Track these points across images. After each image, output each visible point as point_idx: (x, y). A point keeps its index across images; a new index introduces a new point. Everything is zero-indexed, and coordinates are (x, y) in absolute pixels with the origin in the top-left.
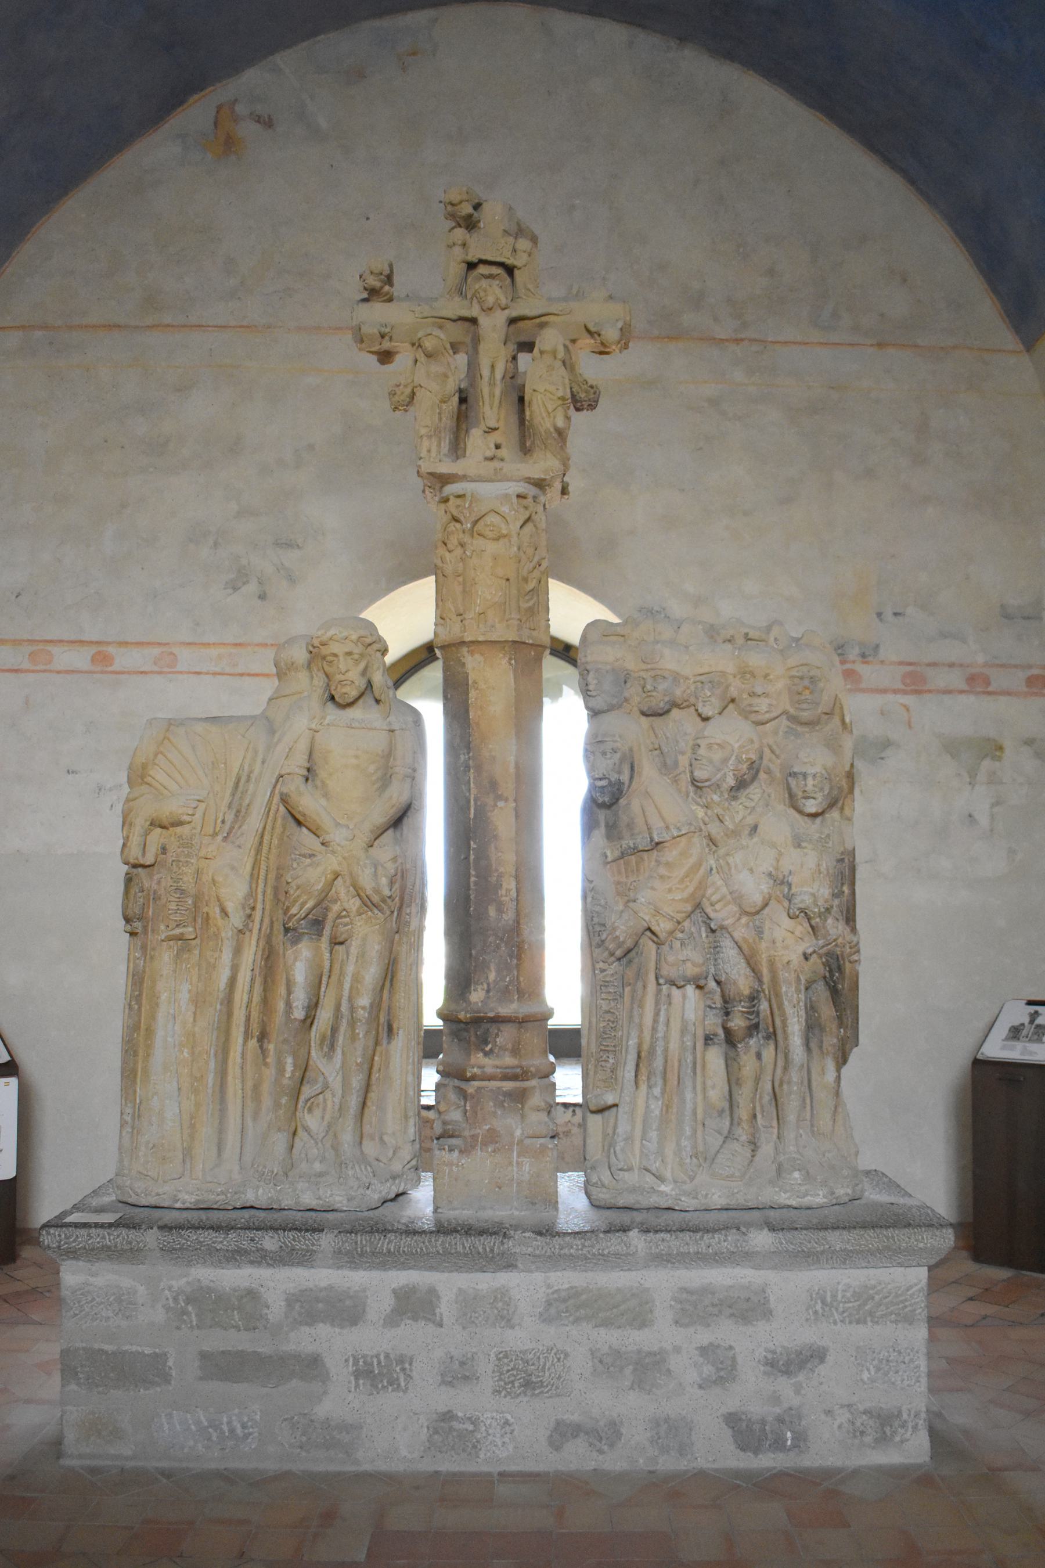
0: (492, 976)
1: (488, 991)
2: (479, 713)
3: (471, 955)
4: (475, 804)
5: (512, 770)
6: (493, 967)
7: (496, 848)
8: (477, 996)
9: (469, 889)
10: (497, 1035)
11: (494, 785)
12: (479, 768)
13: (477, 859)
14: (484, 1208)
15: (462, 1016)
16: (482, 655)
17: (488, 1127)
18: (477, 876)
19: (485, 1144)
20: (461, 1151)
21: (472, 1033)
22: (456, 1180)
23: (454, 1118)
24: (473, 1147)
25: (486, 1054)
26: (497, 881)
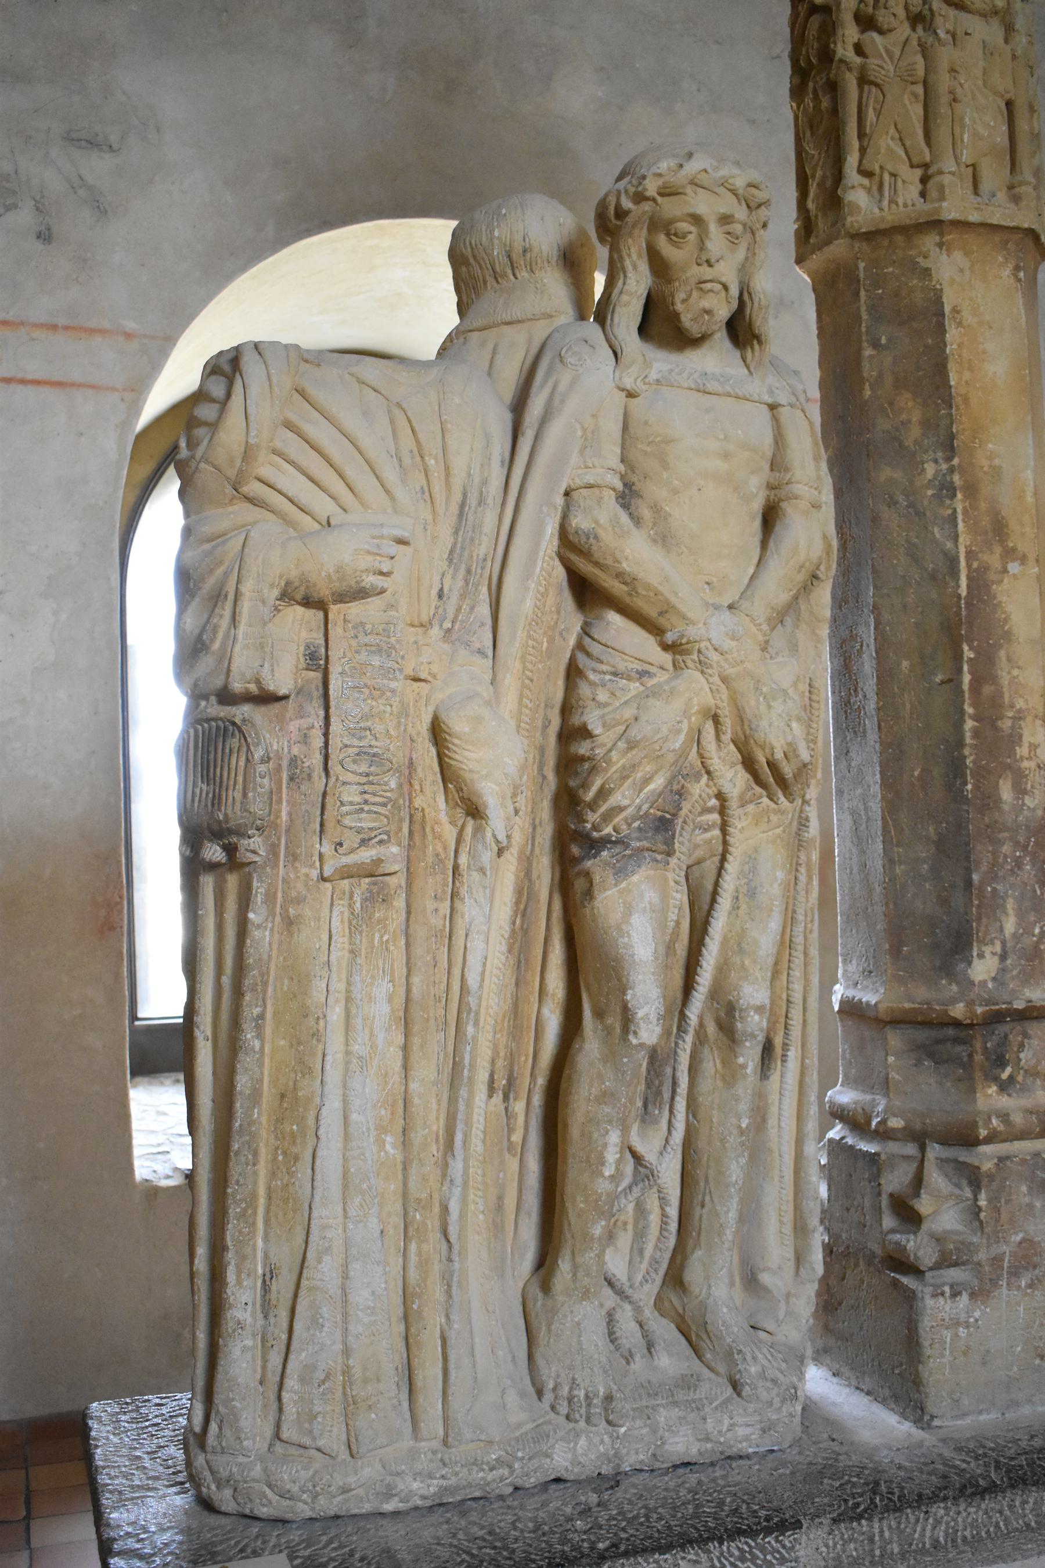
0: (1010, 925)
1: (1003, 957)
2: (967, 375)
3: (969, 883)
4: (969, 566)
5: (1030, 499)
6: (1010, 905)
7: (1009, 660)
8: (983, 968)
9: (960, 744)
10: (1022, 1046)
11: (999, 529)
12: (972, 490)
13: (977, 683)
14: (1015, 1404)
15: (958, 1011)
16: (967, 254)
17: (1019, 1237)
18: (976, 718)
19: (1015, 1273)
20: (973, 1295)
21: (978, 1045)
22: (965, 1354)
23: (948, 1227)
24: (994, 1283)
25: (1004, 1087)
26: (1013, 727)
